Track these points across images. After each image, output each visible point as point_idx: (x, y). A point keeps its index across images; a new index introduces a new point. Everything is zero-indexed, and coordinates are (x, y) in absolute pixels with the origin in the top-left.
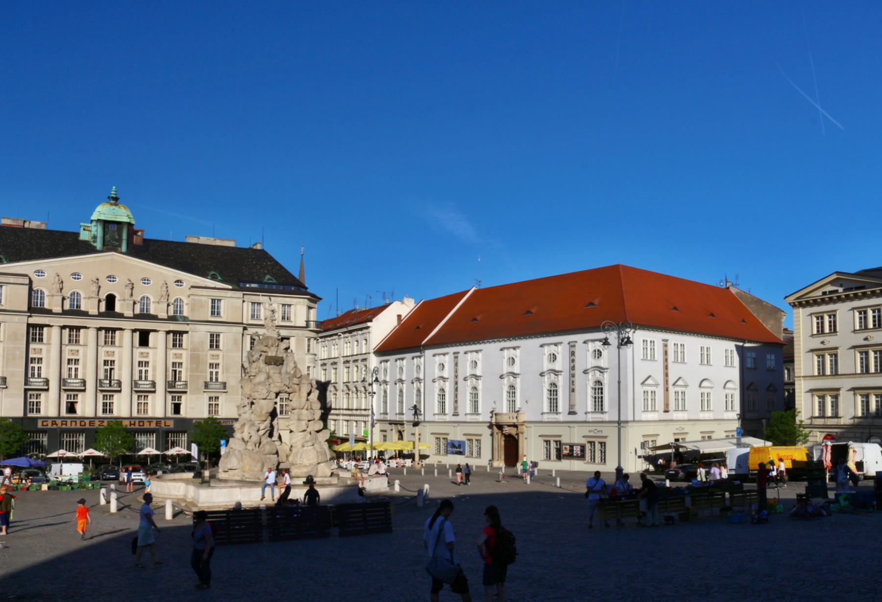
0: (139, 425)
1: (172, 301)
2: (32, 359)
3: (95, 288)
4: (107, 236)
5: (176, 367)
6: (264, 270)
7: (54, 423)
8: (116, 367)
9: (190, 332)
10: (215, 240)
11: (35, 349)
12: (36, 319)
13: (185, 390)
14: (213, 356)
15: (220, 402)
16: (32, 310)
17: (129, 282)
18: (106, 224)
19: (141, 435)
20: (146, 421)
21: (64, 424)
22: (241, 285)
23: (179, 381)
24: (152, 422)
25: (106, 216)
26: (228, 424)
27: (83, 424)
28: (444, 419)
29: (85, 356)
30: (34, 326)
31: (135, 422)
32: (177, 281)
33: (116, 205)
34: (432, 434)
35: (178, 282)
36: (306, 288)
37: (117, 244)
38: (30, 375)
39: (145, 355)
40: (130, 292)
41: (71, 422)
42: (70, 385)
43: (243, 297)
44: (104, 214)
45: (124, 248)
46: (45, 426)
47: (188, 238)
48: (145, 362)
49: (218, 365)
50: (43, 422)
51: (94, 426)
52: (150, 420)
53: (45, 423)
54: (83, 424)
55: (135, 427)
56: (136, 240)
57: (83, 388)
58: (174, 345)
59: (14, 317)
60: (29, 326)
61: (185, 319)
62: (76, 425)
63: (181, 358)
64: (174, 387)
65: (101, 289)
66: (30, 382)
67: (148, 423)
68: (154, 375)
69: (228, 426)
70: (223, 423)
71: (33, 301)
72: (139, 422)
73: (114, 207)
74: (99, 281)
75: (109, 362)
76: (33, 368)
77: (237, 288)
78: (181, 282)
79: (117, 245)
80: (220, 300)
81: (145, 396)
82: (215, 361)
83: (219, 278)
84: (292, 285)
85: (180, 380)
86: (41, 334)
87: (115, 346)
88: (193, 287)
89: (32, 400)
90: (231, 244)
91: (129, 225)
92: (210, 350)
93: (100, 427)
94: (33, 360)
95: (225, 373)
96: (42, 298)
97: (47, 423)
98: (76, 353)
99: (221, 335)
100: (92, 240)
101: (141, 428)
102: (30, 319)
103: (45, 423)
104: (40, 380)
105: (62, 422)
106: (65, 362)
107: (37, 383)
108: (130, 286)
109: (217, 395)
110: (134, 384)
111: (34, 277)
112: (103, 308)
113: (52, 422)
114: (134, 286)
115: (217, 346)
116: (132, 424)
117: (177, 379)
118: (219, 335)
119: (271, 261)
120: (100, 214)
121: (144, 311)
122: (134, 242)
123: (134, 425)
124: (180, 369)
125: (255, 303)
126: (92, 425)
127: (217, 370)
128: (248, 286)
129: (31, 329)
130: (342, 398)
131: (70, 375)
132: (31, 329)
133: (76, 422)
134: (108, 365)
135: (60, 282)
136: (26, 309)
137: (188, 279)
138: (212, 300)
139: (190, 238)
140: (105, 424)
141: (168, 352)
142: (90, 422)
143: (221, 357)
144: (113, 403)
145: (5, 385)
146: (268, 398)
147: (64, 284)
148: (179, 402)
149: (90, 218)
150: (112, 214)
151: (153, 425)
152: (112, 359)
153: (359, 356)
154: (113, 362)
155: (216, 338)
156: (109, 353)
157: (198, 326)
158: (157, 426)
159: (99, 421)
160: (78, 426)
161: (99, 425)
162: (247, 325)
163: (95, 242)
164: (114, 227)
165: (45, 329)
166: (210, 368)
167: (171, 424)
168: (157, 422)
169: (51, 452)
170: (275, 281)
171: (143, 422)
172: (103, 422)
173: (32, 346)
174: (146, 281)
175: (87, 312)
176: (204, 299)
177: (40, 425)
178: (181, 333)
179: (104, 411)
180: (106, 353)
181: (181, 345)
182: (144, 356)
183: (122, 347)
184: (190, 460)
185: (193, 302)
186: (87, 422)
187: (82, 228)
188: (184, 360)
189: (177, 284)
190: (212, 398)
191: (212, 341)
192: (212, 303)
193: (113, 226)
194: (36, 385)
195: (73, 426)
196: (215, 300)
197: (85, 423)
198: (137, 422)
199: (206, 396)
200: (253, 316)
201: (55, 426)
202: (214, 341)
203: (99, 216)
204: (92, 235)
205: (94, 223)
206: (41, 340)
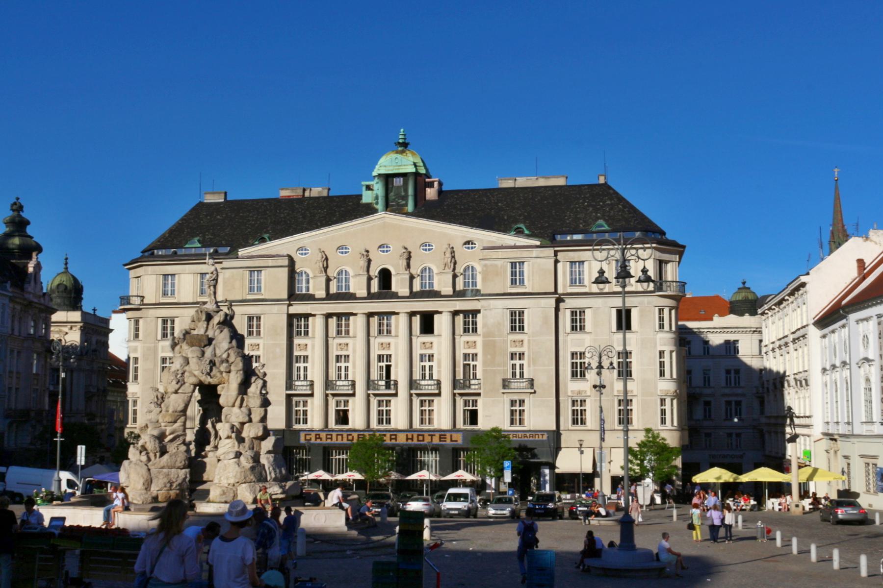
0: (418, 440)
1: (460, 269)
2: (297, 357)
3: (363, 263)
4: (392, 194)
5: (469, 361)
6: (596, 214)
7: (318, 437)
8: (393, 363)
9: (482, 311)
10: (537, 179)
11: (299, 345)
12: (298, 308)
15: (526, 407)
16: (293, 296)
17: (405, 251)
18: (387, 179)
19: (424, 454)
20: (426, 434)
21: (329, 438)
22: (559, 237)
23: (473, 379)
24: (434, 435)
25: (388, 168)
26: (537, 439)
27: (350, 438)
28: (872, 431)
29: (354, 351)
30: (299, 316)
32: (468, 243)
33: (402, 152)
34: (862, 456)
35: (469, 244)
36: (663, 233)
37: (404, 202)
38: (295, 377)
39: (428, 345)
40: (405, 263)
41: (337, 435)
42: (299, 388)
43: (556, 255)
44: (385, 166)
45: (410, 208)
47: (500, 182)
48: (304, 357)
49: (523, 354)
50: (306, 435)
52: (432, 433)
53: (308, 437)
54: (350, 438)
55: (413, 442)
56: (431, 193)
58: (466, 330)
59: (273, 306)
60: (291, 317)
61: (477, 293)
62: (342, 440)
64: (469, 387)
65: (372, 262)
66: (295, 385)
67: (430, 437)
68: (439, 372)
69: (537, 441)
70: (530, 437)
71: (297, 285)
72: (418, 435)
73: (399, 156)
74: (369, 253)
75: (385, 356)
76: (299, 369)
77: (548, 243)
78: (472, 244)
79: (403, 204)
80: (523, 262)
81: (429, 401)
82: (517, 350)
83: (527, 232)
84: (635, 230)
85: (475, 377)
86: (307, 326)
87: (391, 336)
88: (485, 249)
89: (298, 408)
90: (560, 182)
91: (416, 174)
92: (510, 333)
94: (298, 358)
95: (532, 365)
96: (308, 282)
98: (346, 347)
99: (526, 312)
100: (375, 202)
101: (421, 444)
102: (290, 308)
104: (430, 382)
105: (327, 435)
106: (333, 359)
107: (301, 387)
108: (406, 256)
109: (522, 397)
110: (412, 384)
111: (297, 257)
112: (375, 288)
113: (316, 435)
114: (412, 254)
115: (522, 328)
116: (410, 439)
117: (471, 377)
118: (523, 312)
119: (611, 199)
121: (425, 287)
122: (427, 199)
123: (412, 439)
124: (474, 363)
125: (575, 262)
127: (521, 362)
128: (569, 238)
129: (295, 320)
130: (839, 401)
131: (339, 376)
132: (295, 320)
133: (342, 435)
134: (383, 362)
135: (323, 259)
136: (285, 296)
137: (480, 237)
138: (512, 263)
139: (503, 181)
141: (456, 340)
142: (359, 435)
143: (526, 343)
144: (585, 410)
145: (532, 389)
147: (329, 262)
148: (474, 408)
149: (371, 174)
150: (395, 164)
151: (436, 440)
152: (388, 352)
153: (801, 330)
154: (389, 357)
155: (580, 315)
156: (384, 346)
157: (492, 302)
158: (440, 441)
160: (345, 441)
162: (564, 294)
163: (377, 203)
164: (400, 182)
165: (310, 319)
167: (459, 439)
168: (440, 435)
169: (409, 474)
170: (606, 228)
171: (423, 435)
173: (297, 341)
174: (426, 246)
175: (440, 292)
176: (499, 263)
177: (302, 440)
178: (475, 313)
179: (380, 421)
180: (380, 346)
181: (475, 330)
182: (427, 347)
183: (398, 336)
184: (485, 490)
185: (485, 269)
187: (364, 188)
188: (479, 350)
189: (467, 246)
190: (516, 401)
191: (513, 321)
192: (512, 268)
193: (398, 179)
194: (343, 390)
195: (339, 441)
196: (516, 263)
197: (353, 437)
198: (415, 435)
199: (507, 399)
200: (573, 282)
201: (318, 441)
202: (517, 322)
205: (376, 180)
206: (307, 333)
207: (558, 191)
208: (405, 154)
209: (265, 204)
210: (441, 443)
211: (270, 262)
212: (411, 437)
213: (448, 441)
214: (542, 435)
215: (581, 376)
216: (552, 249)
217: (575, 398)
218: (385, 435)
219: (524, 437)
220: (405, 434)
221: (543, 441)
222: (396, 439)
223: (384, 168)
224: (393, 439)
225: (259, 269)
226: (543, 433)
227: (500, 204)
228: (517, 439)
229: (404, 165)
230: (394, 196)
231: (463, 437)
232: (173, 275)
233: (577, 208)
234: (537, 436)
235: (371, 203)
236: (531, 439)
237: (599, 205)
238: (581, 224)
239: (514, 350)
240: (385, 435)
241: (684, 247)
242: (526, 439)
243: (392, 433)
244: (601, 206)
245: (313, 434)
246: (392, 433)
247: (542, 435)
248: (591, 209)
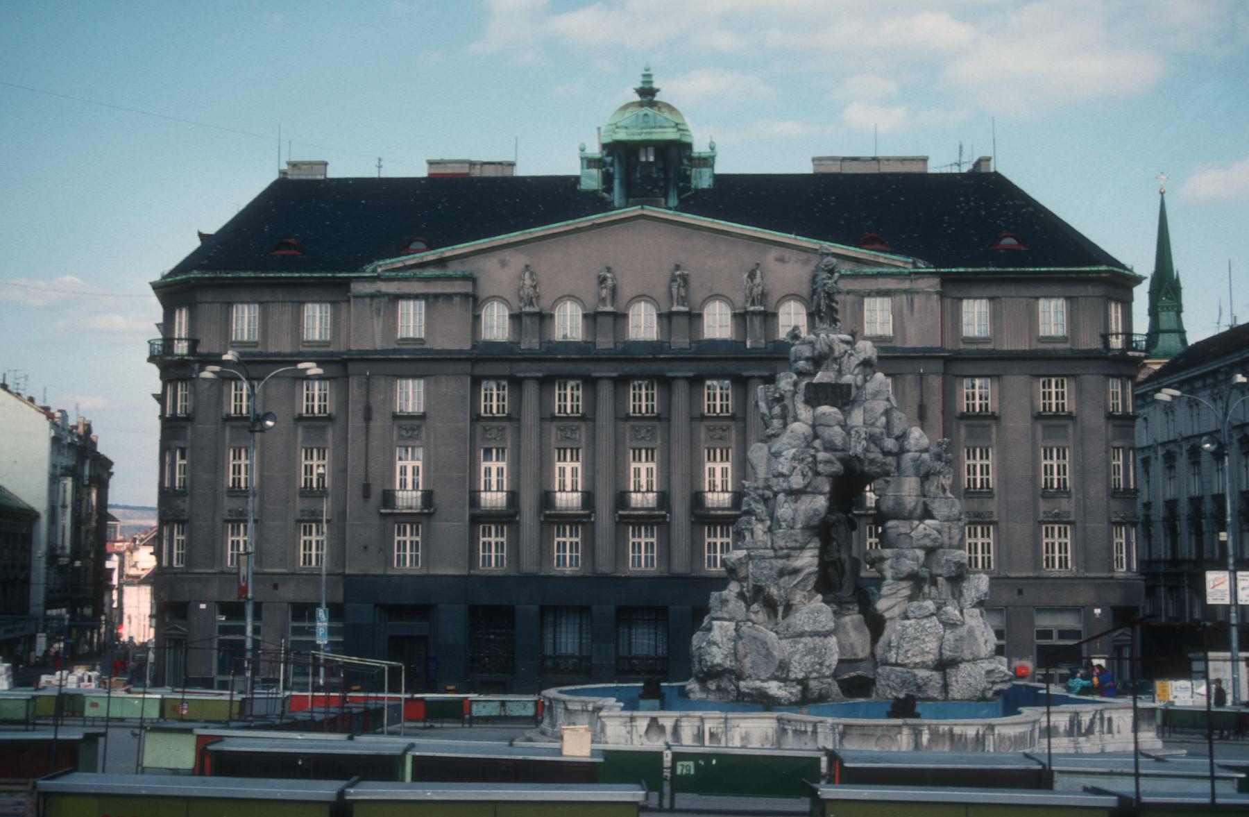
25: (629, 131)
44: (626, 128)
120: (617, 128)
146: (809, 489)
163: (609, 189)
203: (615, 133)
223: (625, 130)
229: (661, 127)
235: (598, 190)
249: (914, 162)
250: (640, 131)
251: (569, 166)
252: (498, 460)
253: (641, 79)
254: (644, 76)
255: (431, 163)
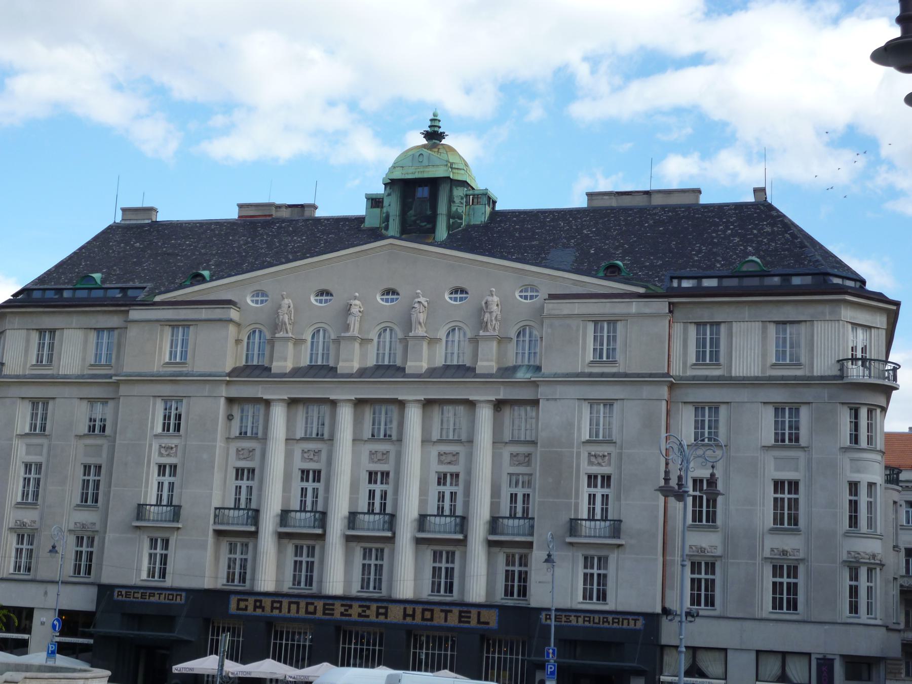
0: (423, 619)
4: (412, 212)
7: (258, 605)
13: (529, 539)
14: (595, 456)
20: (437, 609)
21: (277, 608)
24: (451, 611)
26: (625, 626)
27: (311, 608)
31: (414, 609)
37: (429, 226)
41: (290, 603)
46: (242, 609)
50: (239, 600)
51: (332, 615)
53: (242, 605)
54: (311, 608)
55: (415, 622)
57: (319, 531)
62: (298, 612)
63: (528, 464)
67: (443, 615)
72: (424, 610)
93: (344, 618)
97: (246, 603)
100: (384, 225)
103: (242, 605)
105: (273, 602)
109: (602, 553)
113: (256, 601)
116: (409, 615)
119: (772, 225)
123: (413, 616)
126: (327, 612)
133: (298, 604)
140: (355, 610)
142: (325, 605)
151: (453, 620)
158: (460, 621)
159: (342, 605)
161: (342, 614)
166: (589, 486)
167: (492, 618)
168: (460, 612)
171: (432, 611)
172: (350, 606)
185: (549, 331)
186: (320, 604)
195: (293, 613)
197: (316, 607)
201: (259, 612)
204: (384, 215)
207: (683, 212)
208: (436, 150)
209: (213, 227)
210: (462, 625)
211: (204, 313)
212: (411, 613)
213: (474, 623)
214: (635, 620)
215: (708, 521)
216: (666, 300)
217: (697, 559)
218: (368, 607)
219: (604, 622)
220: (402, 607)
221: (635, 630)
222: (386, 614)
224: (382, 614)
225: (186, 324)
226: (636, 617)
227: (585, 231)
228: (592, 624)
230: (414, 216)
231: (500, 616)
232: (53, 331)
233: (714, 238)
234: (625, 622)
236: (615, 625)
237: (752, 233)
238: (719, 262)
239: (594, 470)
240: (368, 607)
241: (897, 304)
242: (606, 625)
243: (380, 605)
244: (754, 234)
245: (251, 600)
246: (380, 605)
247: (635, 620)
248: (737, 239)
249: (686, 194)
250: (414, 171)
251: (358, 208)
252: (248, 479)
253: (429, 123)
254: (431, 120)
255: (241, 206)
